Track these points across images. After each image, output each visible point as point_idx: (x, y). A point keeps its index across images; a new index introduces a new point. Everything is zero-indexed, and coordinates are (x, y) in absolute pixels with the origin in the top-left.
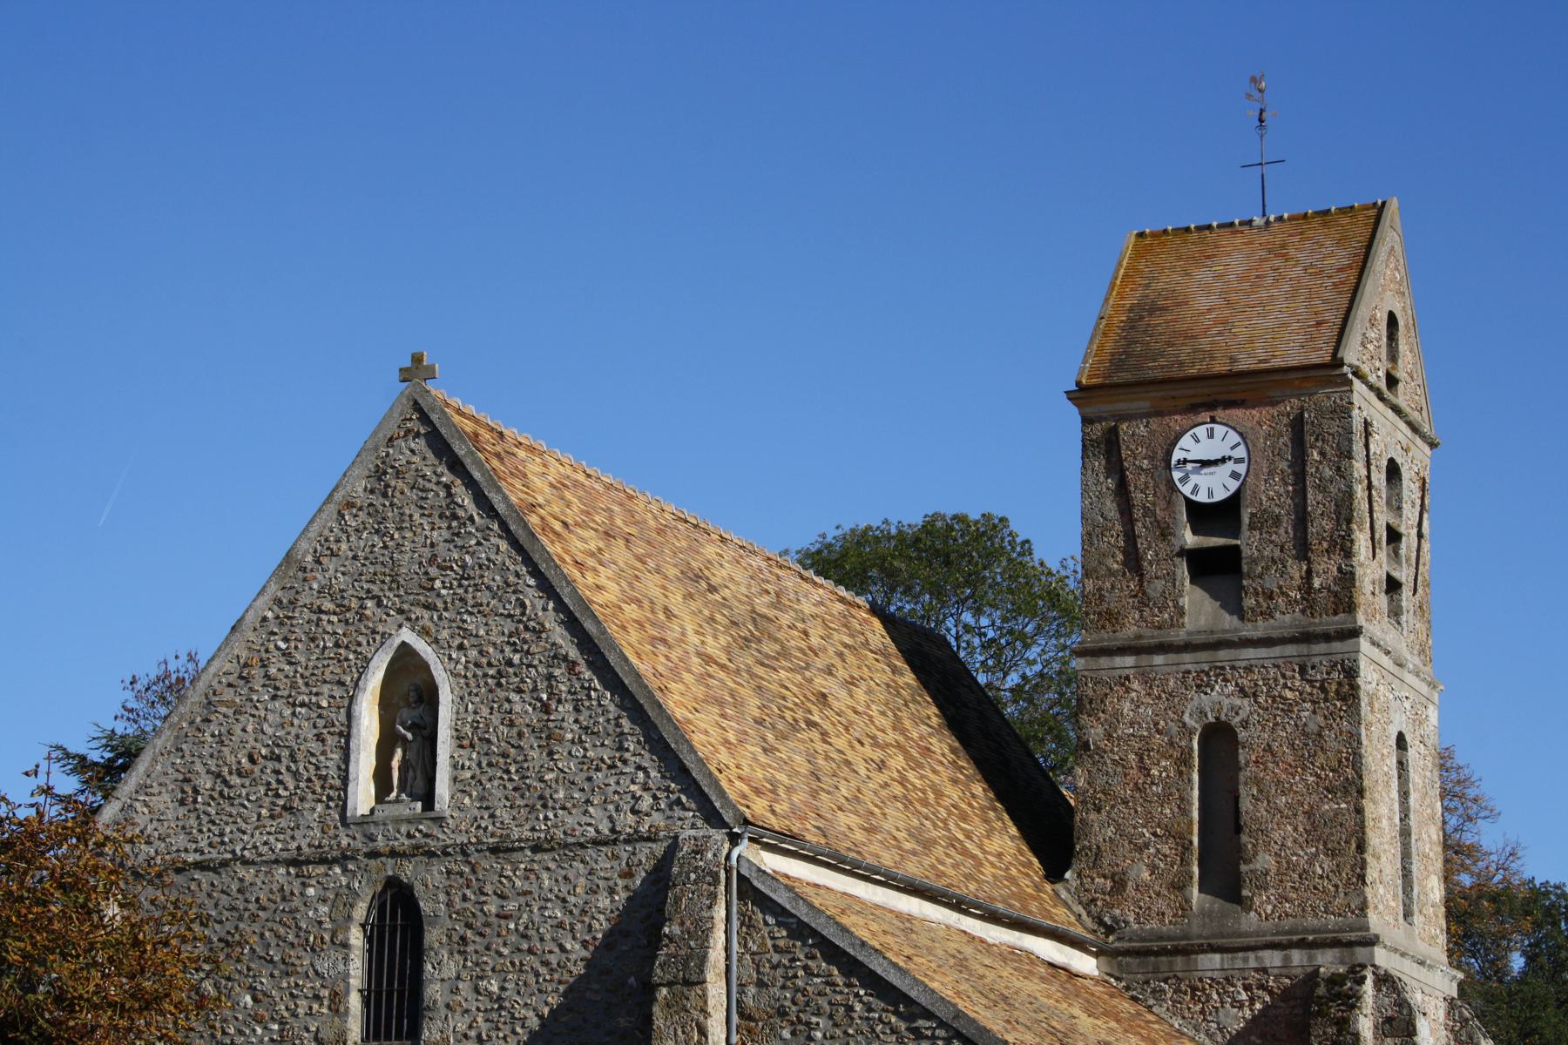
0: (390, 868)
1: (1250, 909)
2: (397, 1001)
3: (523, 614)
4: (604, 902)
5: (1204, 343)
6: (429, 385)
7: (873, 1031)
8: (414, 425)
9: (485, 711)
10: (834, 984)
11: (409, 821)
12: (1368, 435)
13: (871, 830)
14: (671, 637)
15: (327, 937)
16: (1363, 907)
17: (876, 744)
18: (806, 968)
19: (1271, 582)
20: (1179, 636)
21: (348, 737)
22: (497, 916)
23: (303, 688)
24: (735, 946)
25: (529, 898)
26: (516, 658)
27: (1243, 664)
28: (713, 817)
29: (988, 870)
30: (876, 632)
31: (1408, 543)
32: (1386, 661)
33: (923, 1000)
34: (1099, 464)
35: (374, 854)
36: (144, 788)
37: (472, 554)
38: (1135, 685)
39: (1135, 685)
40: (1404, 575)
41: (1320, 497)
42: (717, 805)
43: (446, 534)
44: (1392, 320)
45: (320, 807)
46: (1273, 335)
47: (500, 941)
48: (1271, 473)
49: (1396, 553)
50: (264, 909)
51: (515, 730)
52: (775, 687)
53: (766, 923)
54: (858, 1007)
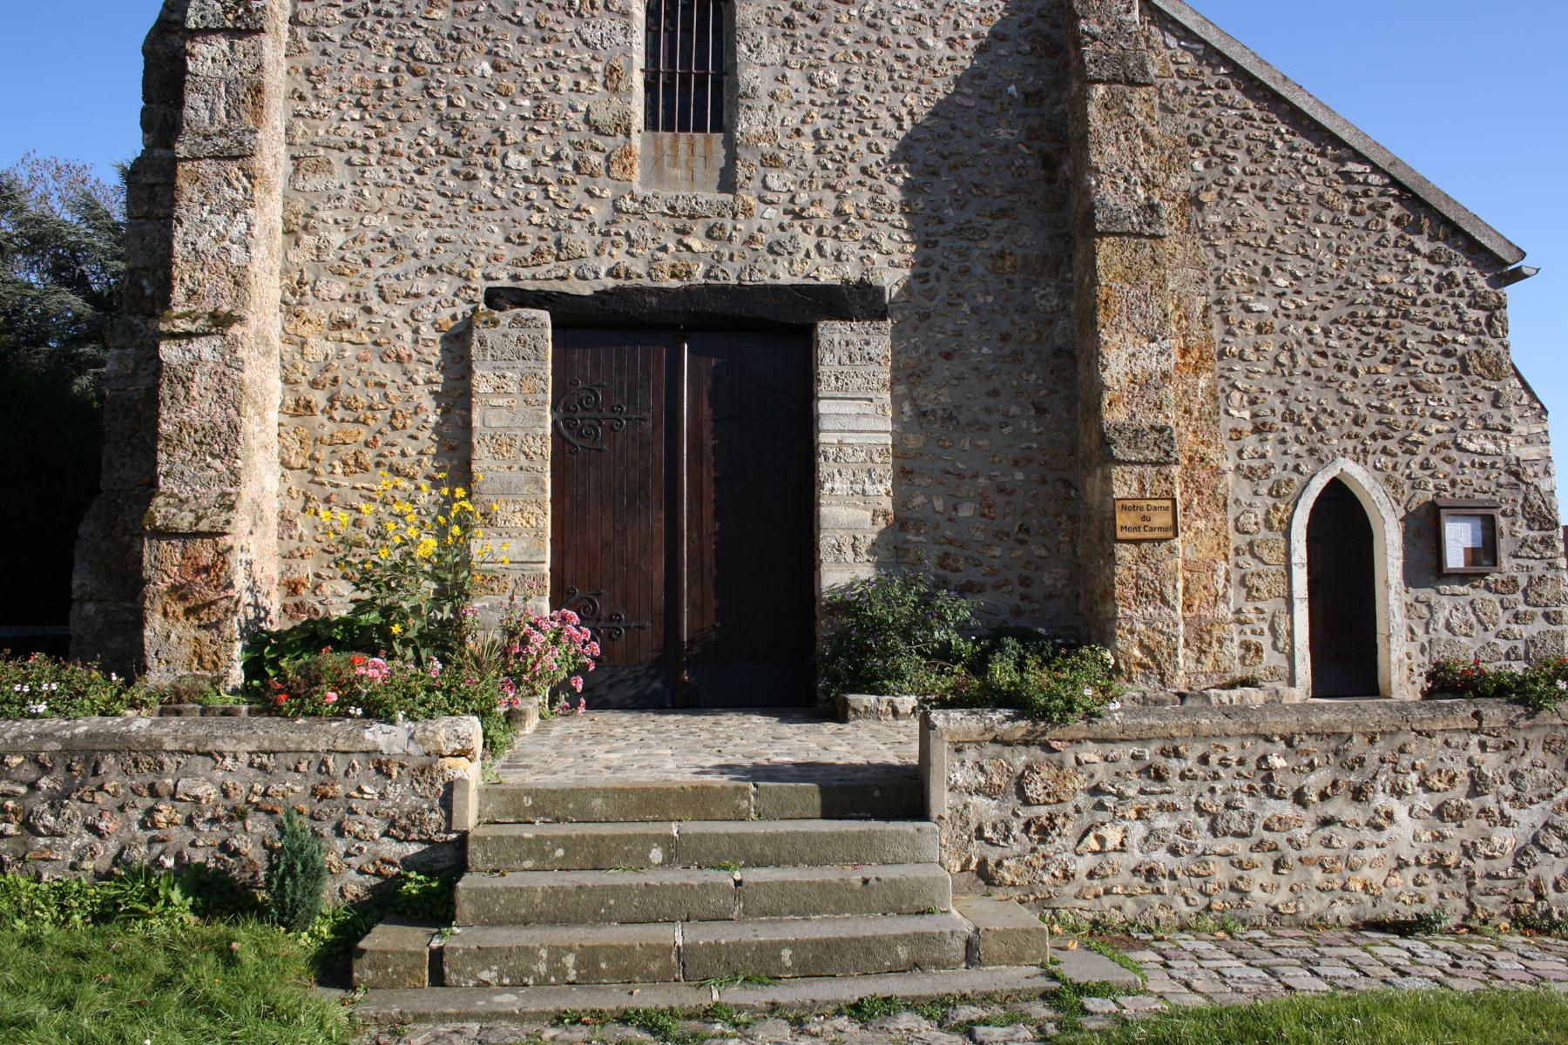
7: (1299, 171)
10: (1251, 118)
18: (1217, 97)
47: (840, 28)
53: (1167, 47)
54: (1279, 144)
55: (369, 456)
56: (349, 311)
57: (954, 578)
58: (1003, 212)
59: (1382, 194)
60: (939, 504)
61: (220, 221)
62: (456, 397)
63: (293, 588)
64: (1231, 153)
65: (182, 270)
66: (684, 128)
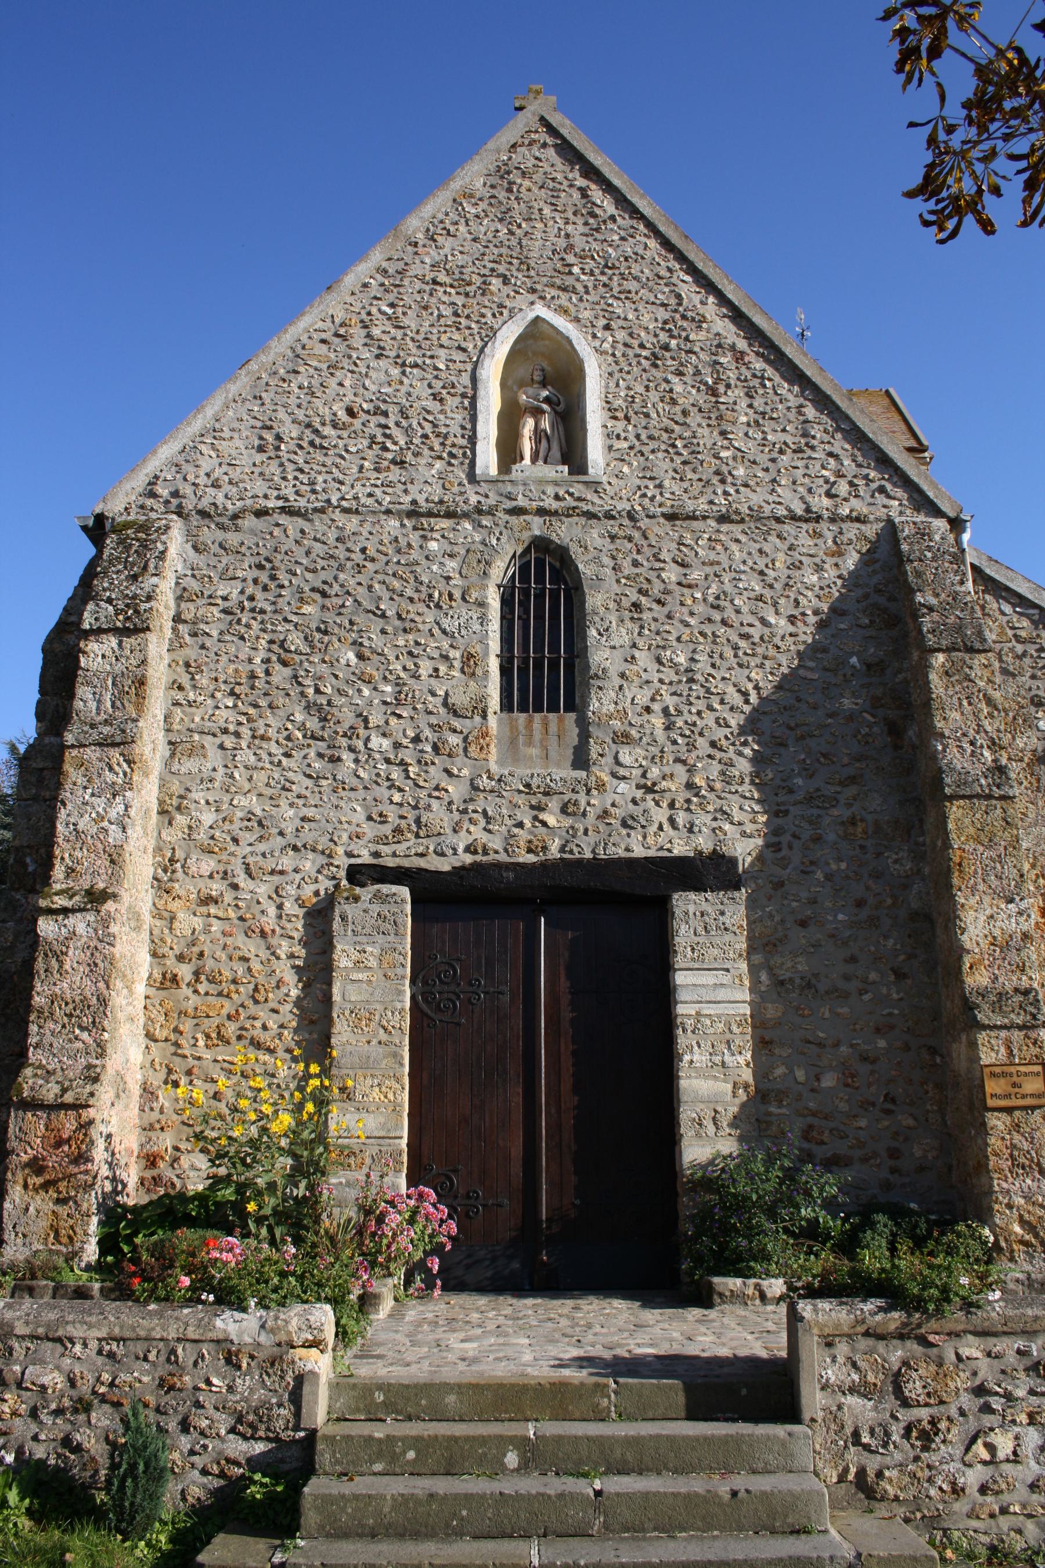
0: (537, 527)
3: (680, 304)
8: (543, 136)
11: (556, 483)
15: (457, 594)
21: (474, 399)
22: (679, 584)
23: (414, 351)
25: (716, 568)
42: (931, 494)
43: (581, 229)
45: (438, 465)
47: (685, 610)
50: (373, 560)
51: (678, 409)
53: (1003, 613)
55: (231, 1029)
56: (216, 887)
57: (820, 1152)
58: (852, 780)
60: (800, 1075)
61: (100, 803)
62: (318, 971)
63: (151, 1160)
65: (63, 849)
66: (538, 709)
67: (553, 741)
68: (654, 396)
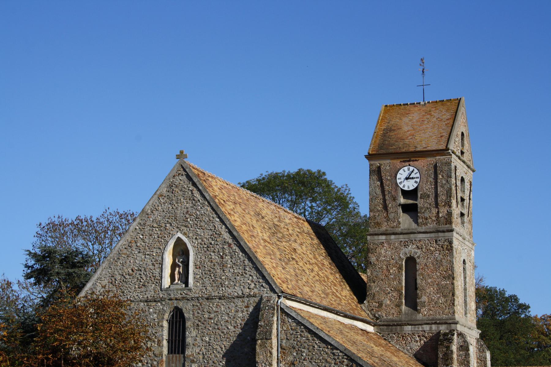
1: (420, 313)
2: (178, 344)
4: (240, 315)
5: (407, 141)
6: (185, 160)
9: (203, 258)
10: (309, 340)
11: (181, 290)
12: (456, 170)
13: (313, 292)
14: (255, 234)
15: (156, 324)
16: (454, 312)
17: (310, 264)
18: (300, 335)
19: (427, 215)
20: (399, 230)
24: (280, 329)
26: (213, 242)
27: (418, 239)
28: (272, 290)
29: (343, 301)
30: (307, 227)
31: (466, 202)
32: (460, 238)
33: (336, 345)
34: (375, 177)
35: (171, 299)
36: (99, 279)
37: (199, 211)
38: (385, 245)
39: (385, 245)
40: (465, 211)
41: (442, 189)
42: (274, 287)
43: (191, 205)
44: (463, 134)
45: (153, 285)
46: (427, 139)
48: (427, 182)
49: (463, 205)
51: (213, 264)
52: (282, 248)
59: (343, 358)
64: (303, 350)
66: (175, 353)
67: (178, 362)
68: (207, 260)
